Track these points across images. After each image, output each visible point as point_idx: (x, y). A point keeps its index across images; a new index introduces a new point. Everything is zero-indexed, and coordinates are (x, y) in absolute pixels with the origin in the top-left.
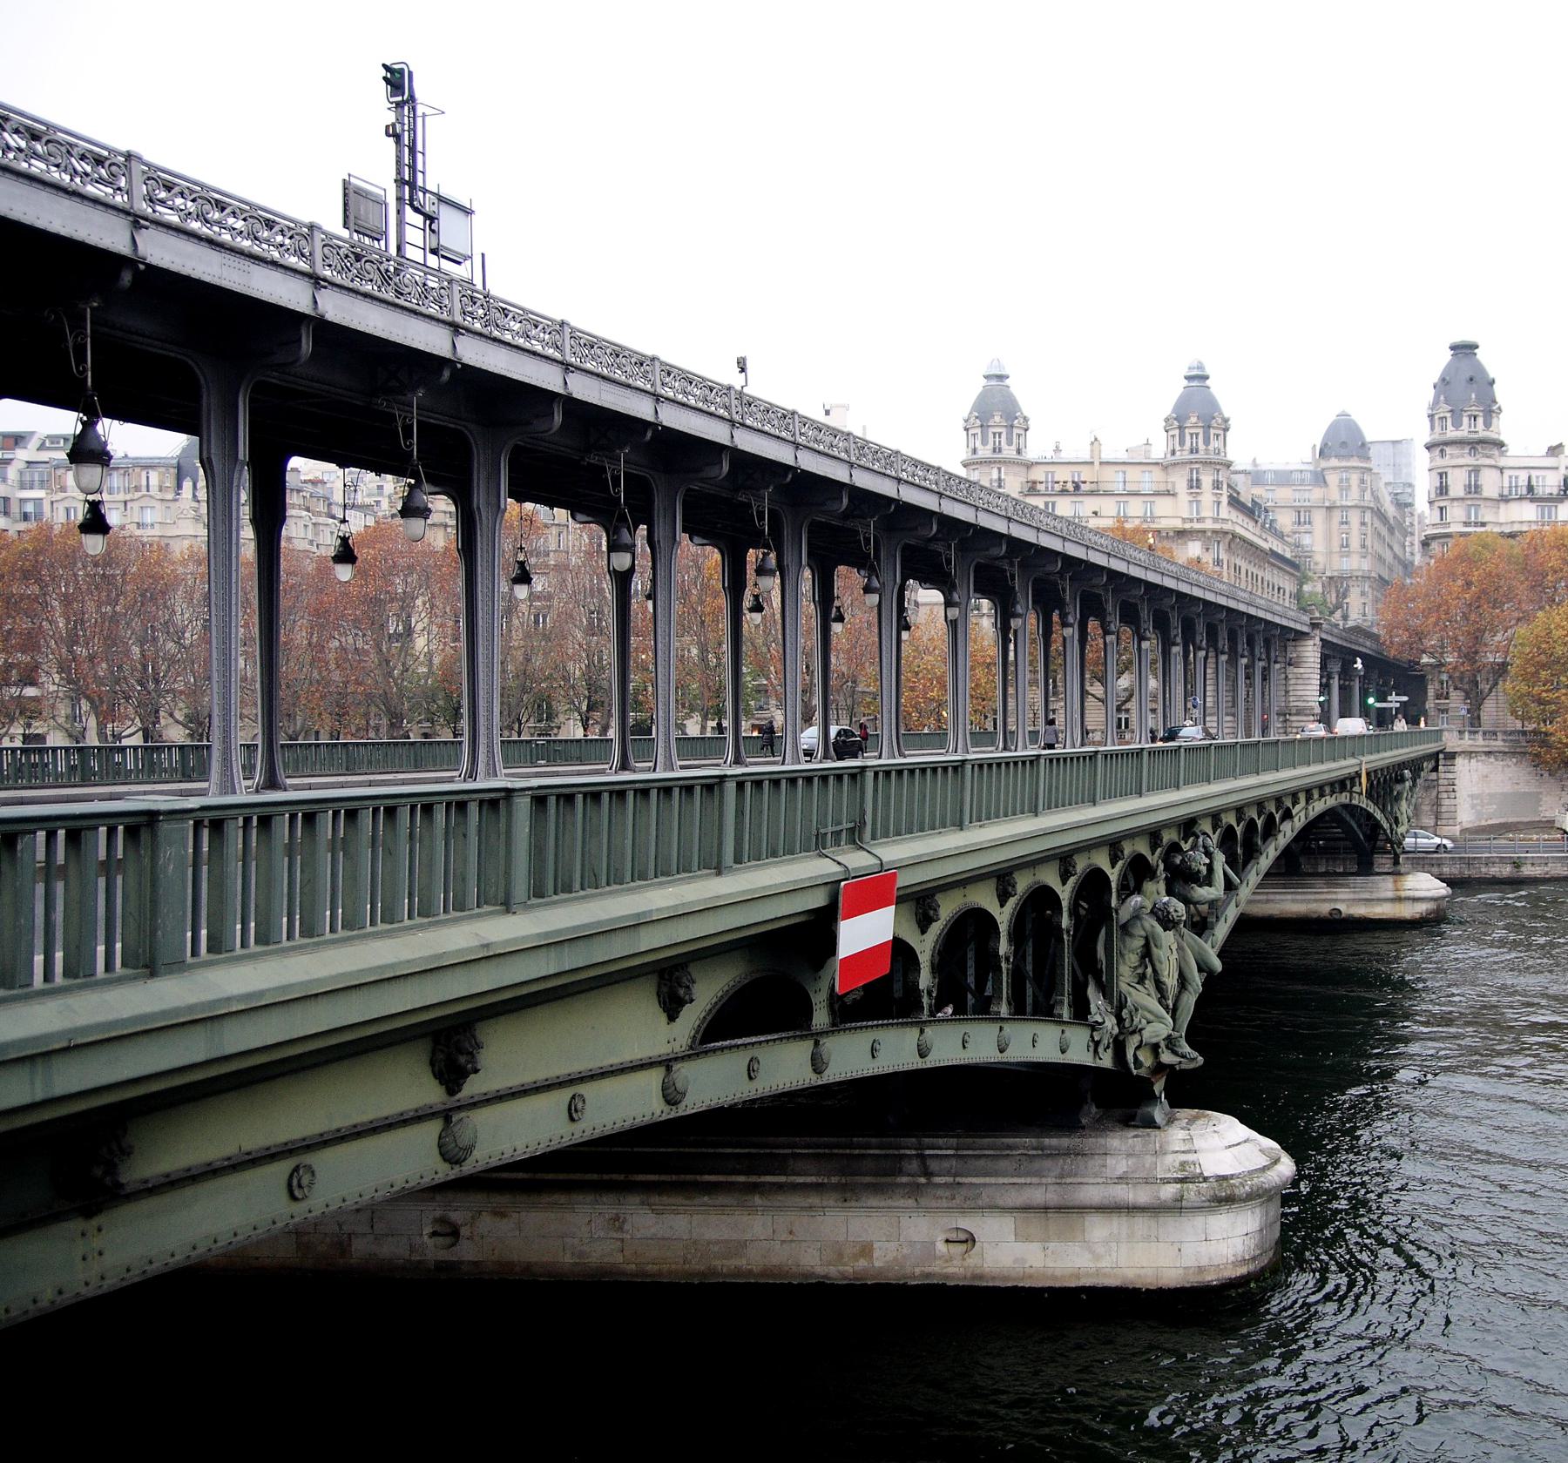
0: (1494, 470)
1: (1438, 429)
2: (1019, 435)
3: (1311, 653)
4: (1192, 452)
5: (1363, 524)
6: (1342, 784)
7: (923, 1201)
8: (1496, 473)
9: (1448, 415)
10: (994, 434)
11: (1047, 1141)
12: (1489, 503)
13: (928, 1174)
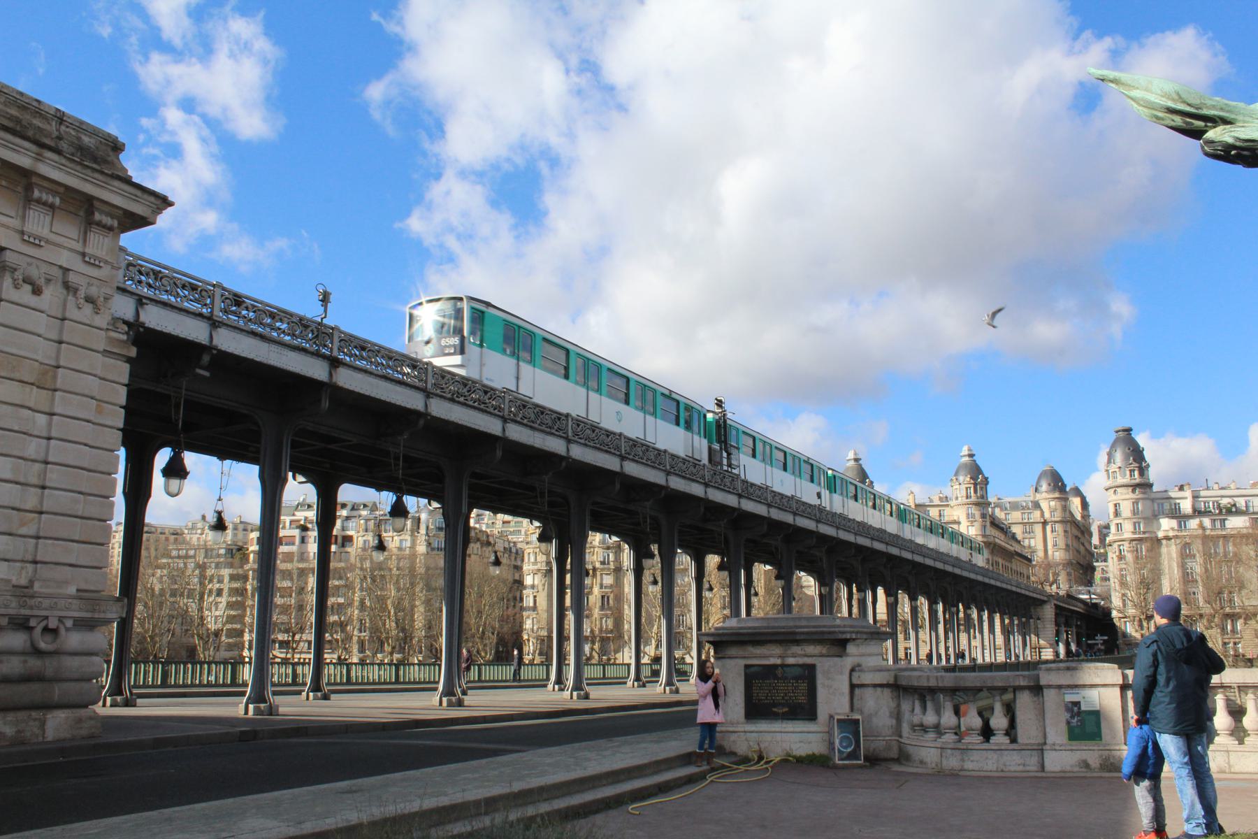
9: (1117, 470)
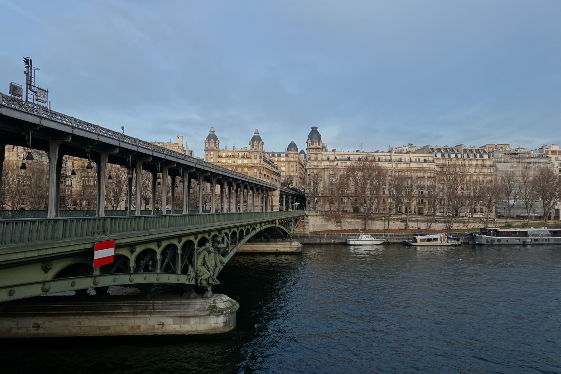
0: (320, 155)
1: (309, 145)
2: (217, 145)
3: (277, 193)
5: (296, 165)
6: (273, 222)
7: (152, 316)
8: (320, 155)
11: (182, 301)
13: (154, 309)
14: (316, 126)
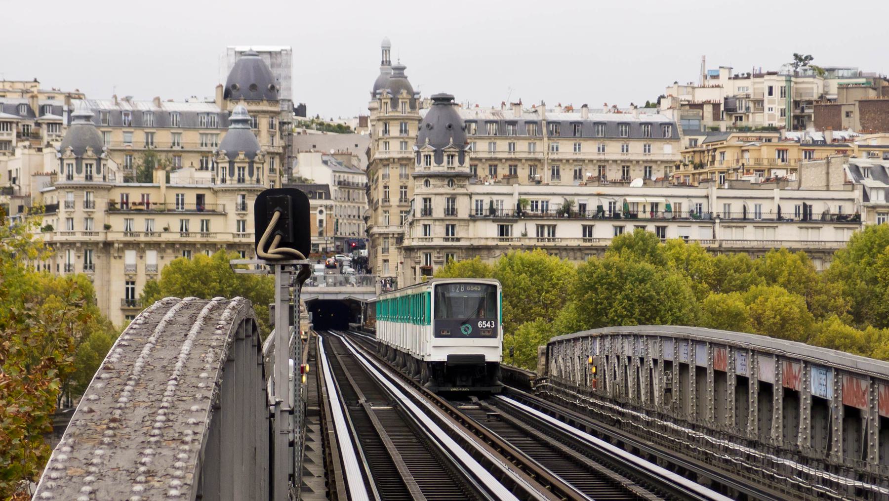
4: (239, 181)
8: (467, 198)
9: (432, 154)
10: (87, 165)
12: (462, 223)
14: (449, 92)
